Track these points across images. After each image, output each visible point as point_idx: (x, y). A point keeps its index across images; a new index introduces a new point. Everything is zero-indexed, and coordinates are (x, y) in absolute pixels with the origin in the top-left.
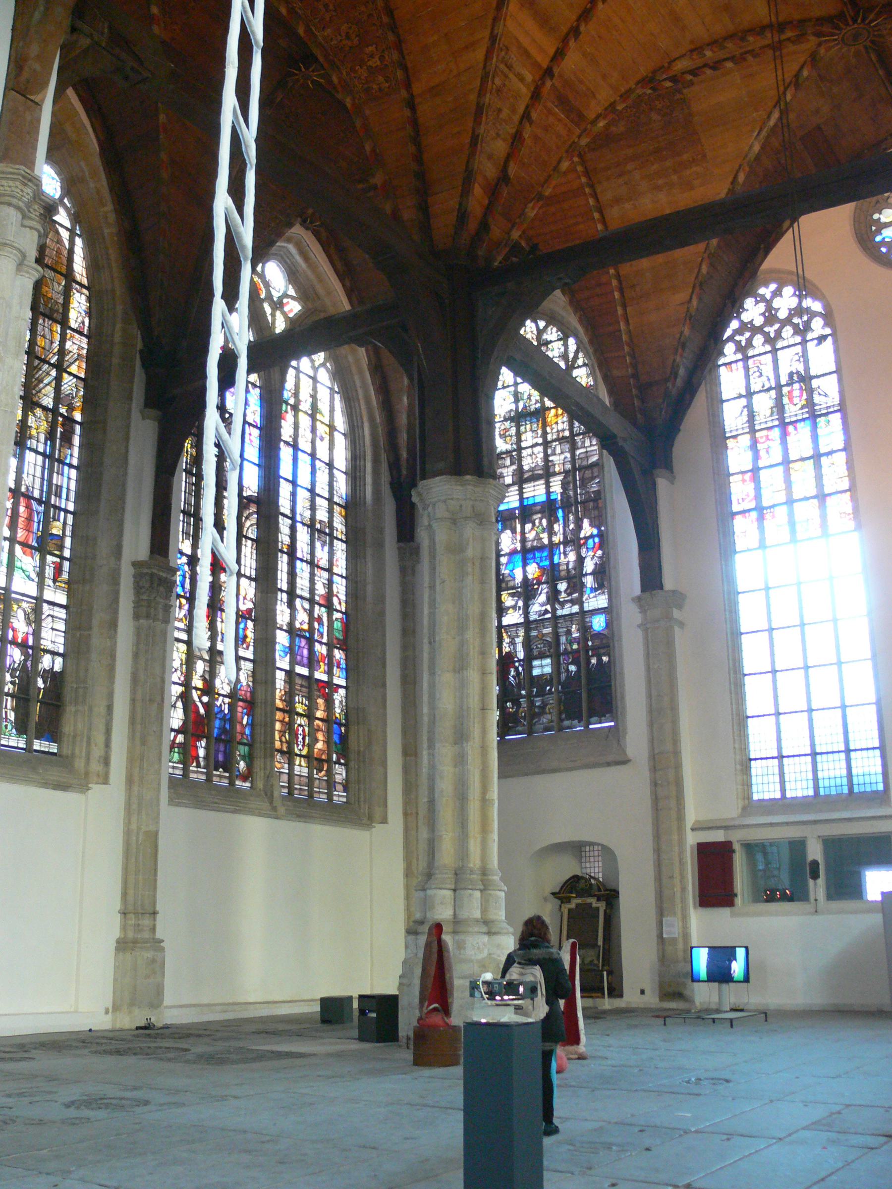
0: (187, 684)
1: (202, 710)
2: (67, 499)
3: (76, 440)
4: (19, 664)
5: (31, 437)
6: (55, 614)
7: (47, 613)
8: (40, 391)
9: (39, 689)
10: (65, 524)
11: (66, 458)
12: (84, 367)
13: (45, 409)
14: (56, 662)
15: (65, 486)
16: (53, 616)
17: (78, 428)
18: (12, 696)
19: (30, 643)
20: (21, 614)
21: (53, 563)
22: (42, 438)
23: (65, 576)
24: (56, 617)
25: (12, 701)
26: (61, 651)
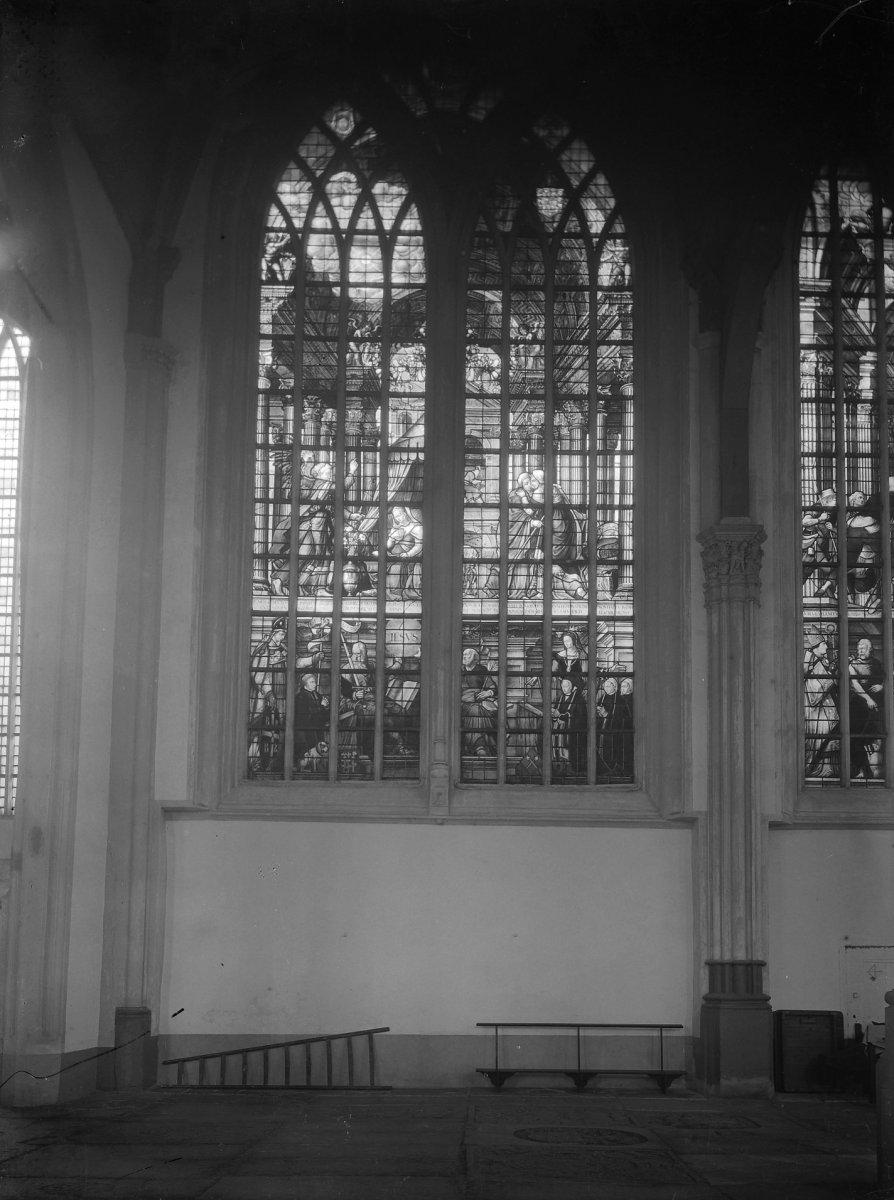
0: (836, 673)
1: (871, 703)
2: (623, 493)
3: (630, 419)
4: (571, 696)
5: (560, 438)
6: (617, 629)
7: (606, 631)
8: (568, 381)
9: (602, 718)
10: (621, 522)
11: (616, 445)
12: (631, 327)
13: (578, 399)
14: (623, 684)
15: (617, 476)
16: (614, 633)
17: (630, 407)
18: (563, 733)
19: (584, 668)
20: (568, 640)
21: (608, 572)
22: (577, 434)
23: (628, 583)
24: (619, 633)
25: (565, 739)
26: (630, 669)
